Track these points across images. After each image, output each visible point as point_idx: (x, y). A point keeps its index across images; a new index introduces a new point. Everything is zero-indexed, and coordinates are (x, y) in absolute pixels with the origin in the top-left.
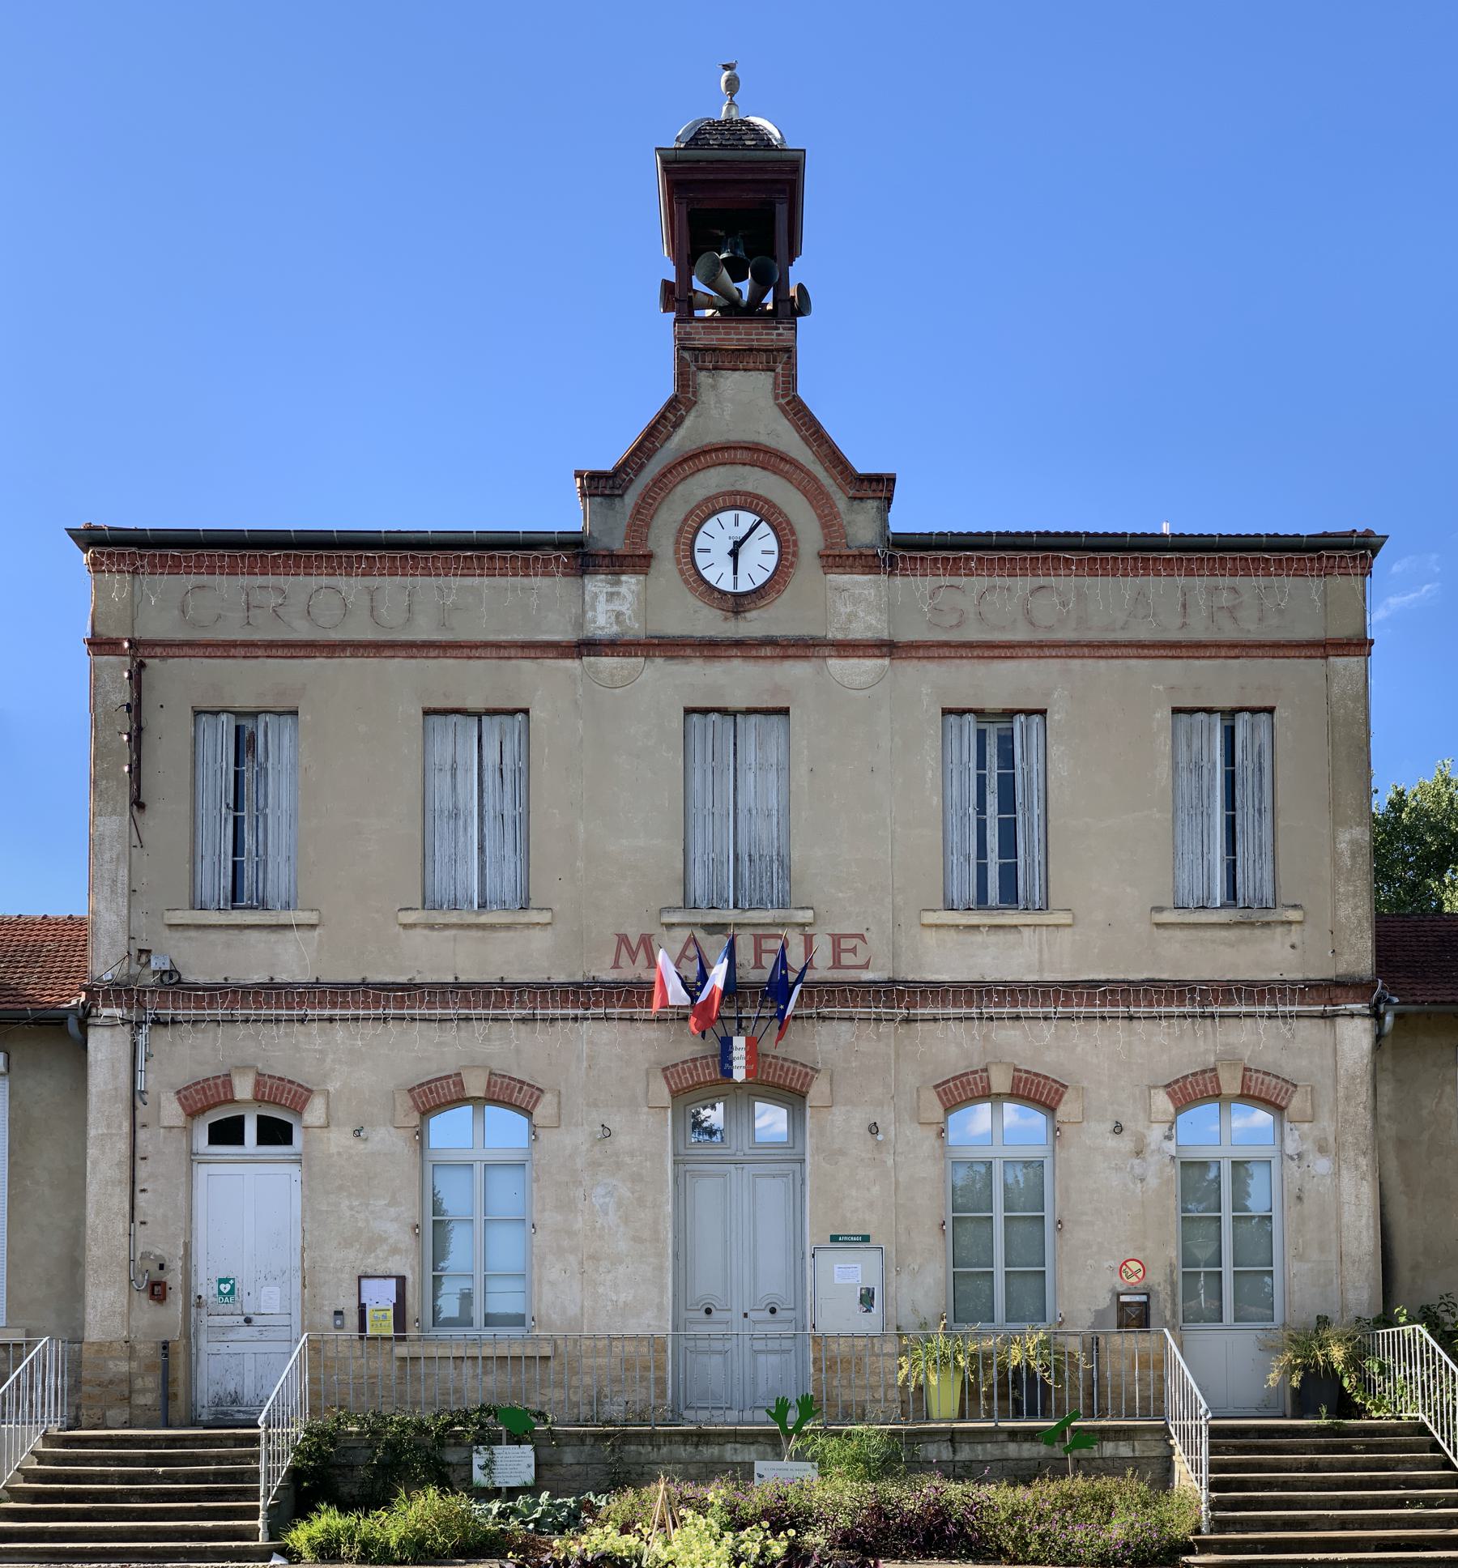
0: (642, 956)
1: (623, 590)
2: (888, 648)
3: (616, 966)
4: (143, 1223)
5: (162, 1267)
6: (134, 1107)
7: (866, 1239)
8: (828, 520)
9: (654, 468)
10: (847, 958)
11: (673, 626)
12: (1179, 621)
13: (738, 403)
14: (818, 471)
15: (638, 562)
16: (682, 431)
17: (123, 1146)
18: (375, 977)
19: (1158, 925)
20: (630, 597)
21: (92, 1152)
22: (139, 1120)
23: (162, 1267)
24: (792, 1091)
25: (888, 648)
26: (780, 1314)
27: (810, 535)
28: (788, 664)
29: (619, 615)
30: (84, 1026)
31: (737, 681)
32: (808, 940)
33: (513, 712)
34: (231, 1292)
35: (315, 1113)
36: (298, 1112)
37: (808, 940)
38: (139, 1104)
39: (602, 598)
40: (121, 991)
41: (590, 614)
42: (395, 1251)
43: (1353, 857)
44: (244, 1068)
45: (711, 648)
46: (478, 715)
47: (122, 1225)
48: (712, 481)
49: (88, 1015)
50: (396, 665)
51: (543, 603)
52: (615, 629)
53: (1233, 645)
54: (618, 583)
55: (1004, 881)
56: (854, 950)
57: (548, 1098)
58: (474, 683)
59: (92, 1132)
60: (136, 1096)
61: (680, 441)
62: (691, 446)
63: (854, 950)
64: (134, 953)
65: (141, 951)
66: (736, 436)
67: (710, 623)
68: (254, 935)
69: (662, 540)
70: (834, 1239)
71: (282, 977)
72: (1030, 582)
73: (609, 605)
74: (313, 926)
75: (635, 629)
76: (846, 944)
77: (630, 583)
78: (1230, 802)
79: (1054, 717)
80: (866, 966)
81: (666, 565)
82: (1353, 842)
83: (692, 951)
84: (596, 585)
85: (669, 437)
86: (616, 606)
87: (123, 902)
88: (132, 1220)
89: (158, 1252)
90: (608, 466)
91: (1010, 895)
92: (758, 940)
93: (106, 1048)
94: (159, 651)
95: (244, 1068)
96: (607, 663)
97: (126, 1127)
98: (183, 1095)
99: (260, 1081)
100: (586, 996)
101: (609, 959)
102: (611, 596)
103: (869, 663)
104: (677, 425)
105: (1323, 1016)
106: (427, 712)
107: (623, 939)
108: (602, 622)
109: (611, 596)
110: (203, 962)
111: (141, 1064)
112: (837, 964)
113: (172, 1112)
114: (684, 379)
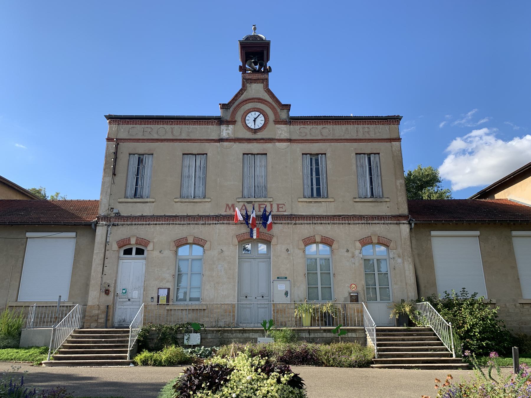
0: (232, 209)
1: (229, 128)
2: (290, 140)
3: (226, 211)
7: (286, 278)
8: (276, 113)
9: (237, 103)
10: (280, 210)
11: (241, 136)
12: (356, 135)
13: (256, 90)
14: (274, 104)
15: (233, 122)
16: (243, 96)
17: (102, 255)
18: (167, 214)
19: (355, 202)
21: (94, 256)
22: (107, 249)
24: (268, 241)
25: (290, 140)
27: (272, 117)
28: (266, 144)
29: (228, 133)
30: (96, 226)
31: (255, 148)
32: (271, 205)
33: (203, 154)
34: (126, 292)
35: (150, 247)
36: (146, 247)
37: (271, 205)
39: (225, 130)
40: (106, 218)
42: (168, 282)
43: (401, 186)
44: (133, 236)
45: (249, 140)
46: (195, 155)
47: (100, 275)
49: (97, 223)
50: (177, 144)
53: (369, 140)
55: (317, 191)
56: (282, 208)
57: (208, 243)
58: (195, 148)
59: (95, 252)
61: (243, 97)
62: (245, 99)
63: (282, 208)
66: (254, 97)
67: (249, 135)
68: (139, 204)
69: (238, 118)
70: (278, 278)
71: (145, 214)
72: (321, 126)
73: (226, 131)
74: (153, 202)
75: (232, 136)
76: (280, 206)
77: (231, 127)
78: (370, 174)
79: (328, 155)
80: (285, 211)
81: (239, 123)
82: (400, 183)
83: (244, 208)
84: (223, 127)
86: (228, 132)
87: (108, 197)
90: (227, 103)
91: (319, 194)
92: (259, 205)
93: (100, 231)
95: (133, 236)
100: (218, 218)
101: (224, 210)
103: (285, 144)
104: (242, 94)
105: (397, 224)
106: (183, 154)
107: (228, 205)
108: (224, 135)
110: (125, 210)
112: (278, 211)
113: (115, 247)
114: (244, 85)
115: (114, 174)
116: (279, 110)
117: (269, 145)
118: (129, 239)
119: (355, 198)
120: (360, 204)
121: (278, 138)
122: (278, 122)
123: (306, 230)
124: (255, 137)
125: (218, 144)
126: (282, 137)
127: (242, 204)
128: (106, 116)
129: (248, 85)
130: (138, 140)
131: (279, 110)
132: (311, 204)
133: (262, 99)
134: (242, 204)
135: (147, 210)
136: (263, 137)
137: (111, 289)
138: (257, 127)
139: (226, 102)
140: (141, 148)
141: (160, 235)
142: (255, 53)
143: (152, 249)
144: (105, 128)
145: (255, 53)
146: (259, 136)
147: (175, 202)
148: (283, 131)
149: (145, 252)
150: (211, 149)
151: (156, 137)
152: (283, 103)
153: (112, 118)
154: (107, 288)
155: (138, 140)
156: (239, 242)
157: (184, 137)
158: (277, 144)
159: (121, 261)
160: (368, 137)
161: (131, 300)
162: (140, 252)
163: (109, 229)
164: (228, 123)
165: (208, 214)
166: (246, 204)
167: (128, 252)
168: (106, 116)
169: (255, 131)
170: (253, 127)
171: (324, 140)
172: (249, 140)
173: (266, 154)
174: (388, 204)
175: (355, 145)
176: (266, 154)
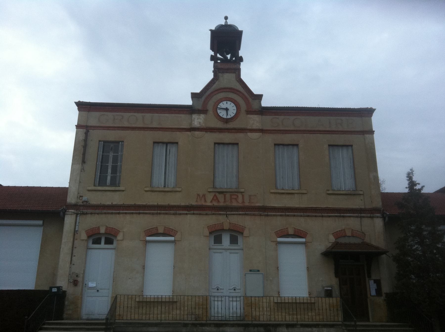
1: (201, 117)
3: (197, 201)
4: (73, 264)
5: (77, 276)
6: (74, 235)
7: (258, 271)
9: (209, 92)
13: (227, 79)
16: (215, 85)
17: (70, 245)
20: (202, 119)
21: (63, 246)
22: (75, 238)
23: (77, 276)
26: (237, 291)
29: (200, 122)
30: (64, 215)
35: (120, 237)
36: (116, 237)
38: (76, 234)
39: (196, 119)
40: (75, 206)
41: (193, 122)
45: (220, 130)
46: (167, 144)
47: (68, 265)
48: (222, 95)
49: (66, 211)
51: (183, 121)
52: (199, 125)
54: (200, 116)
59: (63, 241)
60: (75, 232)
61: (215, 87)
64: (79, 196)
65: (80, 196)
67: (220, 125)
68: (108, 193)
69: (210, 107)
70: (250, 271)
73: (198, 120)
74: (123, 191)
75: (204, 125)
77: (202, 116)
79: (301, 146)
81: (211, 112)
83: (215, 198)
84: (195, 116)
85: (212, 86)
86: (199, 120)
88: (71, 263)
89: (77, 272)
92: (231, 195)
94: (92, 128)
96: (197, 133)
97: (72, 239)
98: (87, 232)
99: (107, 228)
102: (198, 119)
104: (214, 84)
105: (370, 217)
106: (154, 143)
107: (198, 195)
109: (198, 119)
110: (95, 199)
111: (77, 224)
113: (84, 236)
115: (84, 162)
116: (250, 100)
117: (241, 135)
118: (99, 228)
119: (328, 190)
120: (333, 197)
121: (250, 128)
122: (250, 112)
123: (279, 222)
124: (226, 126)
125: (189, 133)
126: (255, 127)
127: (213, 194)
128: (76, 103)
129: (220, 75)
130: (108, 128)
131: (250, 100)
132: (284, 196)
133: (234, 89)
134: (213, 194)
135: (116, 199)
136: (235, 127)
137: (80, 279)
138: (229, 117)
139: (198, 90)
140: (112, 136)
141: (130, 226)
142: (226, 41)
143: (122, 239)
144: (74, 116)
145: (226, 41)
146: (230, 125)
147: (146, 191)
148: (255, 121)
149: (115, 242)
150: (181, 137)
151: (126, 124)
152: (255, 92)
153: (81, 105)
154: (76, 278)
155: (108, 128)
156: (211, 233)
157: (155, 125)
158: (249, 134)
159: (90, 252)
160: (341, 129)
161: (100, 291)
162: (109, 241)
163: (78, 218)
164: (199, 112)
165: (178, 204)
166: (217, 194)
167: (97, 241)
168: (76, 103)
169: (227, 121)
170: (225, 117)
171: (297, 131)
172: (220, 130)
173: (237, 144)
174: (362, 197)
175: (328, 136)
176: (237, 144)
